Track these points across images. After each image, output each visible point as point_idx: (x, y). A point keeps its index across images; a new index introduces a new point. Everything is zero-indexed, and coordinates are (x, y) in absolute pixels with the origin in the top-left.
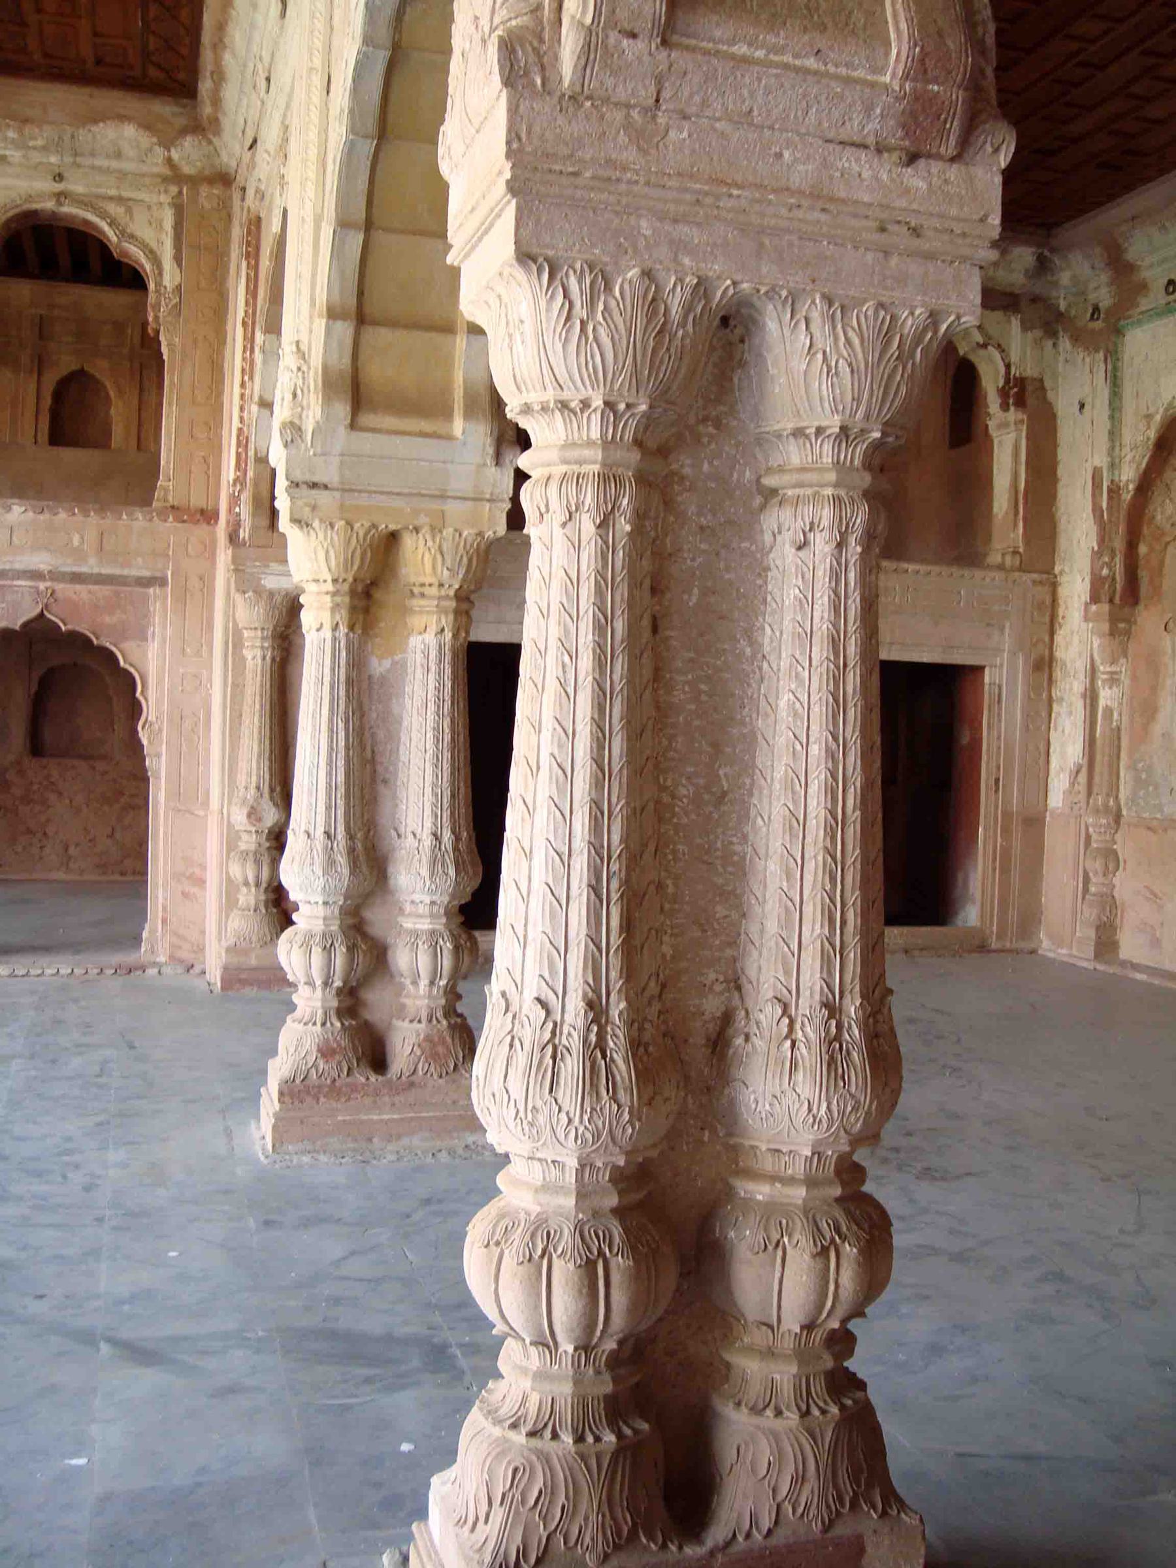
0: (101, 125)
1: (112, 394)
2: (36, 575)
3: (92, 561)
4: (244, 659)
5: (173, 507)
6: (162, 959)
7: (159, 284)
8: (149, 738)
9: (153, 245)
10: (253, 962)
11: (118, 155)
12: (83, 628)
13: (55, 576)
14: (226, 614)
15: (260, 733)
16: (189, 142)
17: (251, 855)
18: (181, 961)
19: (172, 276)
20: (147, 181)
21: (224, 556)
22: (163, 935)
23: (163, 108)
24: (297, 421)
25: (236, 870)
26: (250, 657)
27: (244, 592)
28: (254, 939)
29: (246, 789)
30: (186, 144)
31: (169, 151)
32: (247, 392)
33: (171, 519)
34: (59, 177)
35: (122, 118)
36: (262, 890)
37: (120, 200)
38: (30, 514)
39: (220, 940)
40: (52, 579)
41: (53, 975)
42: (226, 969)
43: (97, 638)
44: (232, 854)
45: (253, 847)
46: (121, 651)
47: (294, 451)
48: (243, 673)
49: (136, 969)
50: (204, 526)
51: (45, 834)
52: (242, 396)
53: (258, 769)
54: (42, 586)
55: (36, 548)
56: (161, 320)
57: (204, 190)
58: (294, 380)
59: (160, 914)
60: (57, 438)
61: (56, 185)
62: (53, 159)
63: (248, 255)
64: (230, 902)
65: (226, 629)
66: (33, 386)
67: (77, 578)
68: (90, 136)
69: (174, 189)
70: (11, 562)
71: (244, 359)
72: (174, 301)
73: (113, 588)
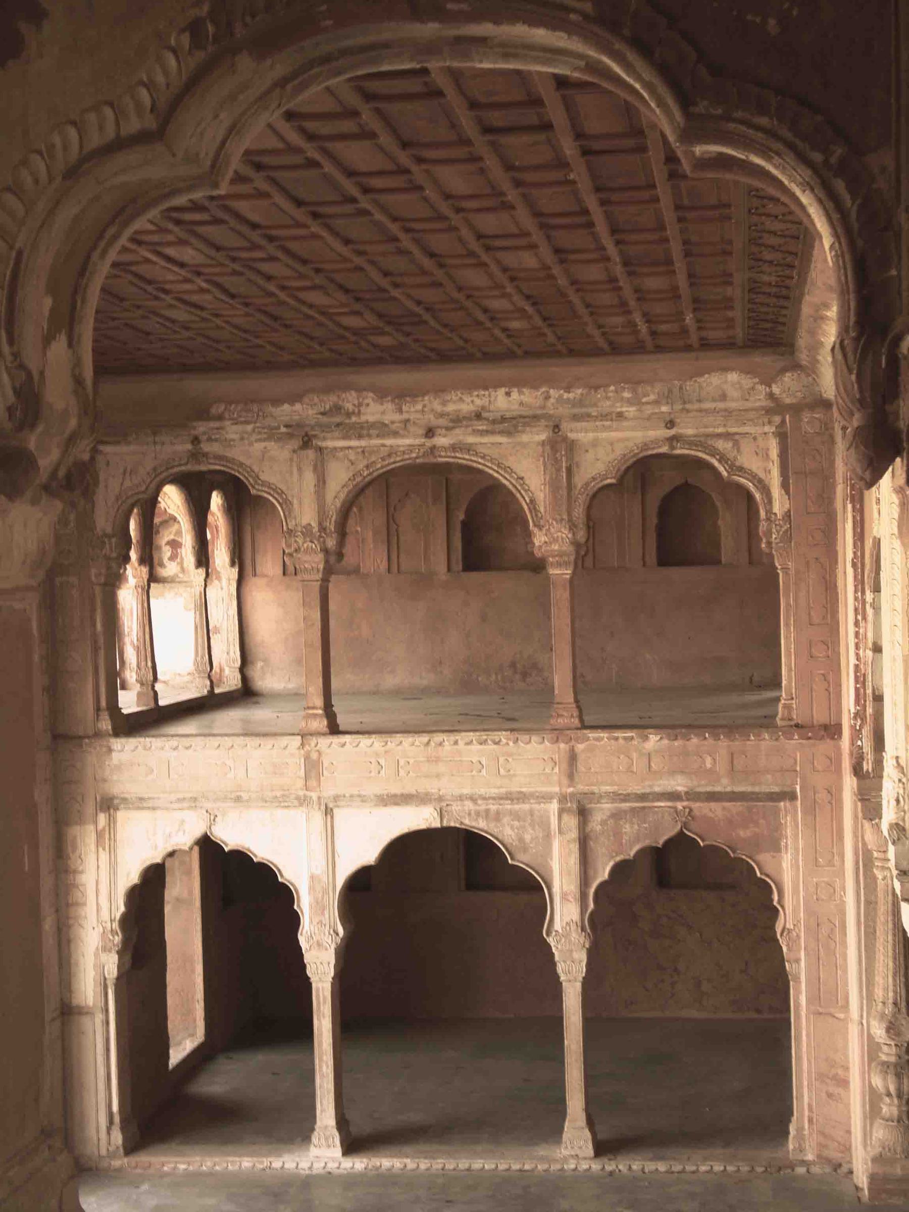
0: (707, 376)
1: (718, 504)
2: (674, 796)
3: (725, 781)
4: (875, 878)
5: (797, 726)
6: (810, 1157)
7: (769, 511)
8: (788, 945)
9: (762, 475)
10: (899, 1171)
11: (724, 397)
12: (719, 842)
13: (692, 796)
14: (855, 835)
15: (894, 951)
16: (788, 378)
17: (892, 1068)
18: (829, 1161)
19: (782, 503)
20: (752, 415)
21: (849, 783)
22: (810, 1134)
23: (764, 360)
24: (901, 823)
25: (877, 1081)
26: (880, 877)
27: (871, 820)
28: (899, 1149)
29: (884, 1003)
30: (786, 379)
31: (770, 387)
32: (861, 631)
33: (796, 737)
34: (671, 424)
35: (725, 370)
36: (904, 1102)
37: (727, 436)
38: (666, 742)
39: (865, 1146)
40: (688, 800)
41: (707, 1172)
42: (873, 1178)
43: (734, 852)
44: (873, 1065)
45: (893, 1059)
46: (758, 865)
47: (900, 847)
48: (875, 889)
49: (787, 1167)
50: (828, 740)
51: (676, 970)
52: (857, 634)
53: (895, 986)
54: (679, 805)
55: (672, 773)
56: (774, 545)
57: (806, 416)
58: (897, 790)
59: (806, 1113)
60: (665, 559)
61: (668, 431)
62: (664, 409)
63: (853, 501)
64: (873, 1112)
65: (856, 854)
66: (637, 510)
67: (712, 797)
68: (697, 385)
69: (777, 419)
70: (651, 786)
71: (856, 599)
72: (785, 528)
73: (745, 804)
